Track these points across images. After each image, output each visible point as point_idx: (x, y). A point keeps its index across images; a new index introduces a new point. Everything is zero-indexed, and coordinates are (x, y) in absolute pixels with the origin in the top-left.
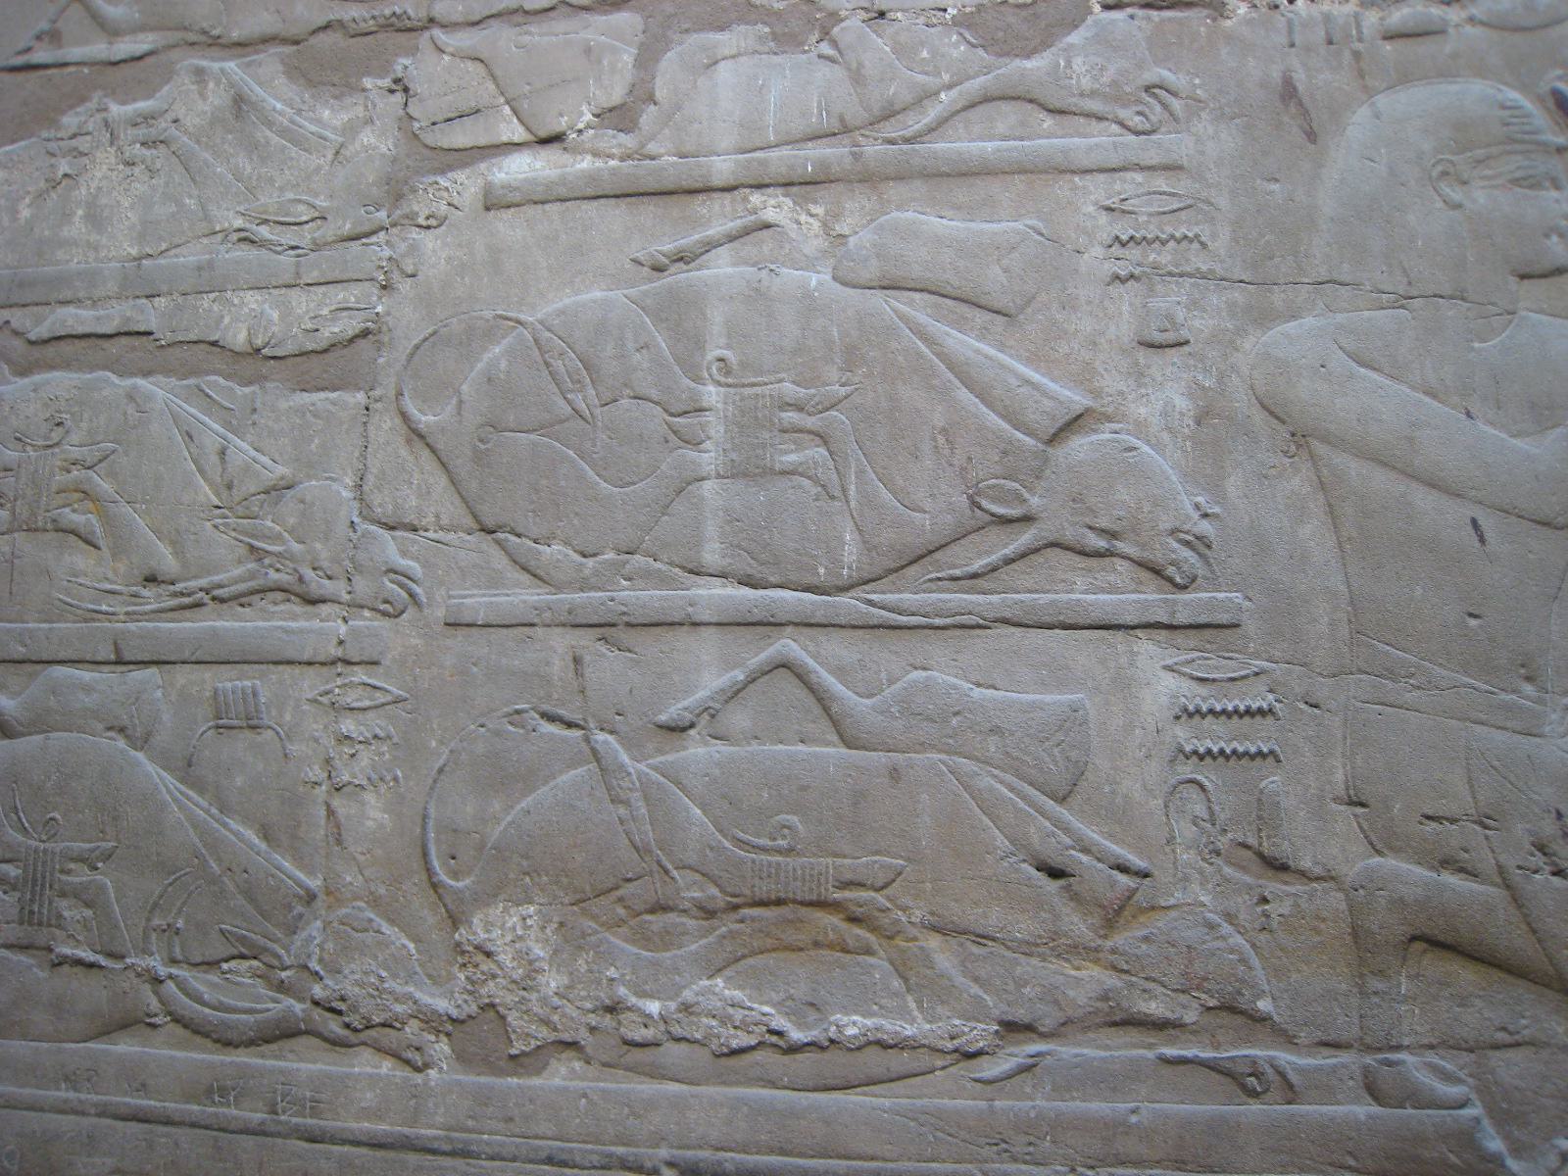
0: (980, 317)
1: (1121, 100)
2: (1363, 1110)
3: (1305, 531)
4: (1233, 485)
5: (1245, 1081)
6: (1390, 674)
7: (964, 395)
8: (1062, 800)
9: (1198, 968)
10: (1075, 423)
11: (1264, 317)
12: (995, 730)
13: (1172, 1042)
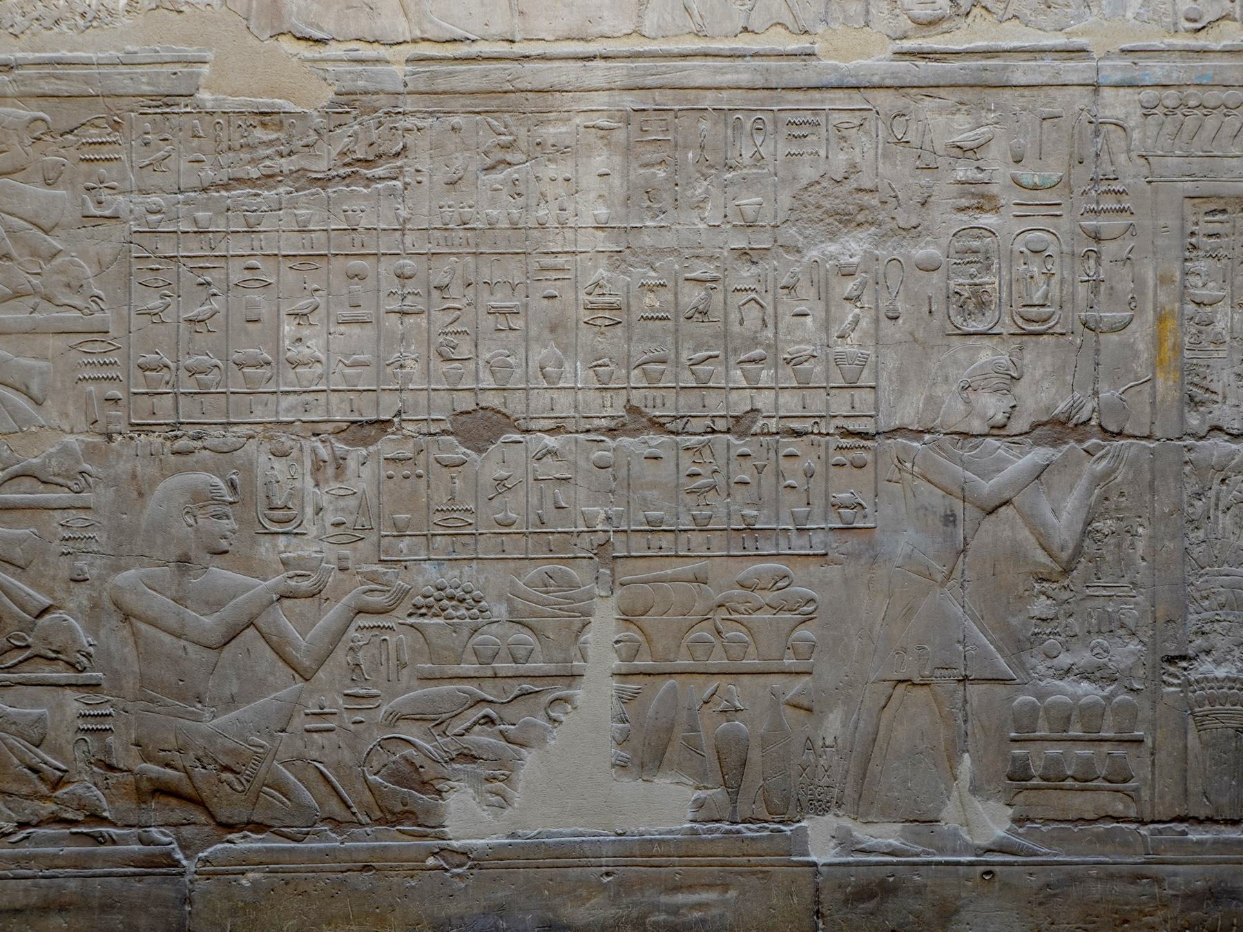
0: (12, 569)
1: (68, 477)
2: (137, 847)
3: (126, 650)
4: (102, 633)
5: (97, 839)
6: (152, 701)
7: (6, 599)
8: (37, 747)
9: (83, 802)
10: (46, 611)
11: (117, 569)
12: (14, 723)
13: (76, 827)
